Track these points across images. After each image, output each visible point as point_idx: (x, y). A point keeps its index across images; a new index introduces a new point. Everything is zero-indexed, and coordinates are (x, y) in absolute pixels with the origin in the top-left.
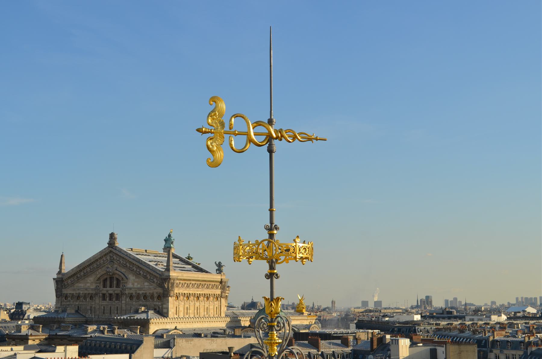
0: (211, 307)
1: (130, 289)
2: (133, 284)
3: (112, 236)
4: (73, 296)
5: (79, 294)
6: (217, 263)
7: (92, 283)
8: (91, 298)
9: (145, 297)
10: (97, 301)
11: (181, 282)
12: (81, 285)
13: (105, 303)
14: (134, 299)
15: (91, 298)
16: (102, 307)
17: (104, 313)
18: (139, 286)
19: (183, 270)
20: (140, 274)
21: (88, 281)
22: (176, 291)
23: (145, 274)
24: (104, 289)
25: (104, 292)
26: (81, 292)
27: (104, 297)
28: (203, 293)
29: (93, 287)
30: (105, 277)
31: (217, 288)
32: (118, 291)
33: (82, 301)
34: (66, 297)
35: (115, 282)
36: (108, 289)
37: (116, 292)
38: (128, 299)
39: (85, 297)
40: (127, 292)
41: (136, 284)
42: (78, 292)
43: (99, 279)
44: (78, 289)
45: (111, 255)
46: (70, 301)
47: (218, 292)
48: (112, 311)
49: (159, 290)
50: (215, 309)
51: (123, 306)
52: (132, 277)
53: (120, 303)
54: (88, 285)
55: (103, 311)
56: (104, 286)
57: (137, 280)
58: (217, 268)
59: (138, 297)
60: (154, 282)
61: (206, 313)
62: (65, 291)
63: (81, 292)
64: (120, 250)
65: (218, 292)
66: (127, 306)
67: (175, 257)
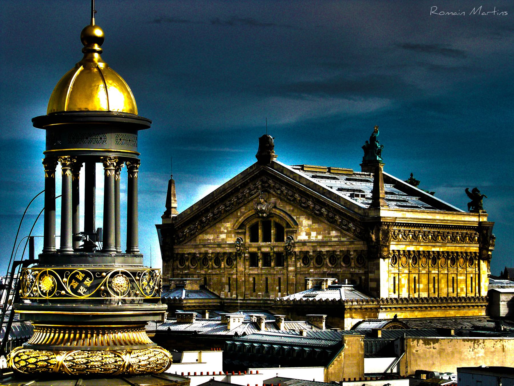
0: (461, 278)
1: (304, 243)
2: (308, 234)
5: (206, 253)
6: (470, 190)
10: (241, 268)
11: (402, 229)
15: (230, 262)
16: (251, 279)
17: (254, 291)
18: (320, 237)
19: (402, 205)
20: (321, 214)
22: (393, 247)
23: (331, 215)
24: (254, 244)
26: (210, 251)
27: (253, 260)
28: (445, 249)
30: (254, 221)
31: (472, 240)
32: (279, 247)
33: (213, 268)
36: (261, 243)
37: (275, 250)
40: (297, 250)
41: (314, 234)
42: (203, 250)
43: (242, 226)
44: (204, 246)
46: (188, 268)
47: (474, 248)
50: (469, 282)
52: (305, 222)
54: (223, 236)
55: (252, 286)
56: (254, 238)
57: (316, 226)
58: (470, 200)
59: (319, 258)
60: (349, 230)
61: (451, 290)
63: (210, 251)
65: (474, 248)
66: (298, 276)
67: (388, 180)
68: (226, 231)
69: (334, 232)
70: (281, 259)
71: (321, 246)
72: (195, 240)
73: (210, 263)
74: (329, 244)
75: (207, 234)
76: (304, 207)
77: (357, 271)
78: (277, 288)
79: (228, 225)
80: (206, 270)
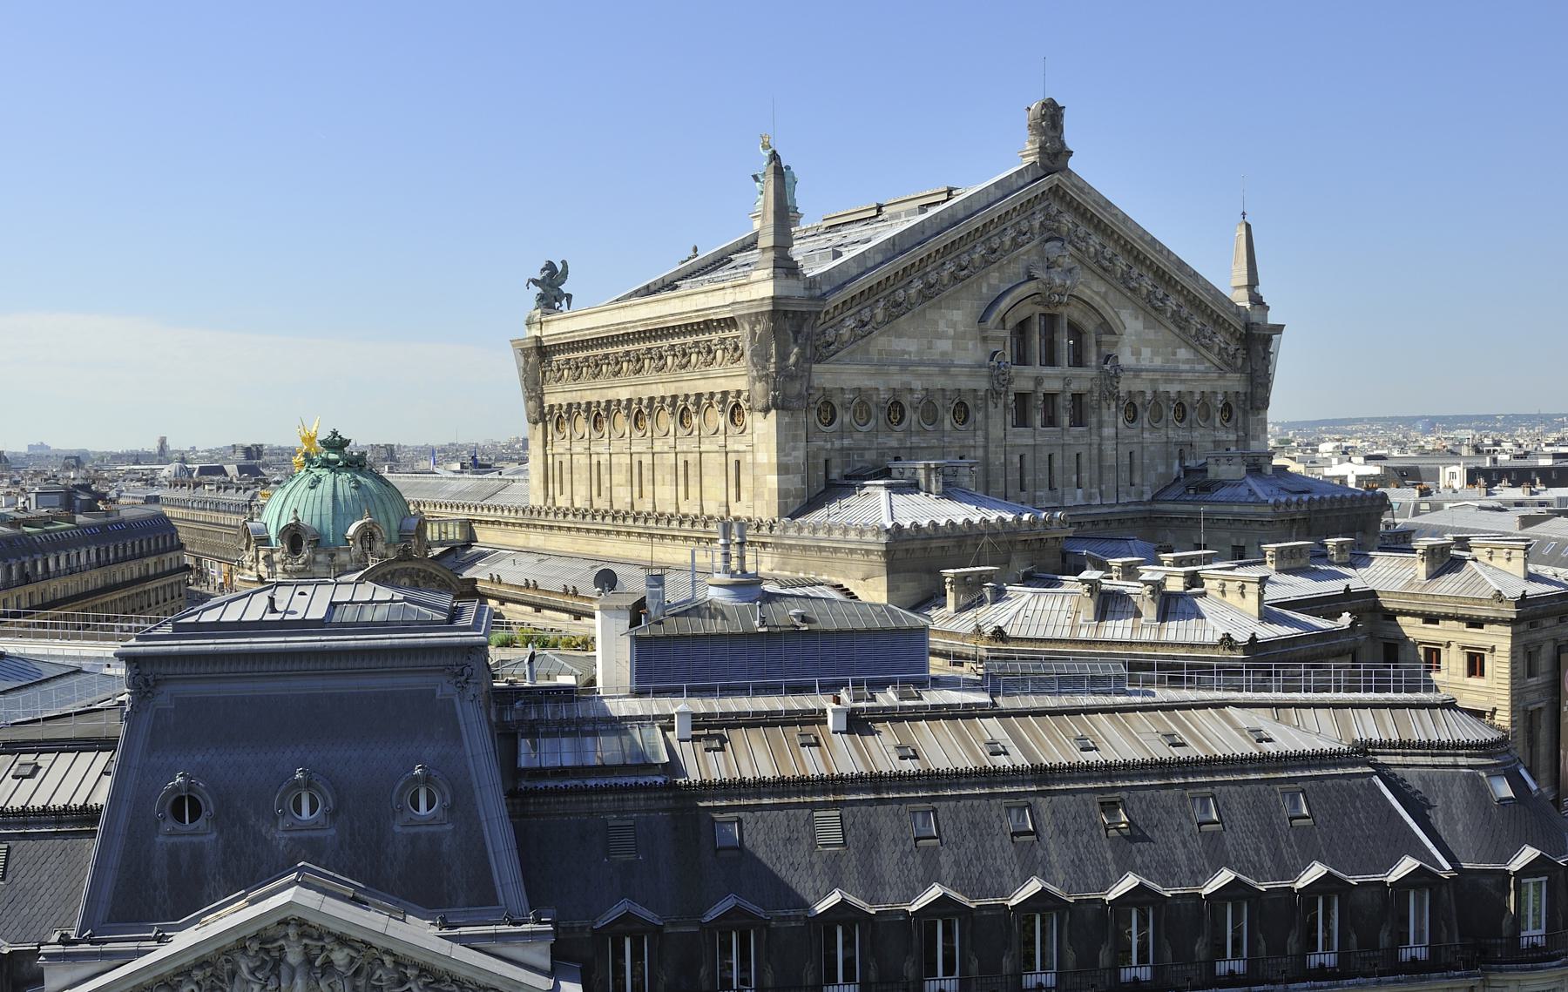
2: (1136, 353)
3: (1051, 118)
4: (862, 403)
7: (963, 336)
8: (962, 412)
9: (1181, 410)
10: (996, 432)
12: (906, 345)
13: (1024, 437)
14: (1146, 417)
15: (962, 412)
16: (1016, 459)
18: (1158, 361)
21: (942, 327)
25: (1025, 385)
26: (917, 384)
29: (972, 353)
30: (1025, 311)
32: (1084, 379)
34: (828, 411)
35: (1065, 342)
37: (1074, 387)
38: (1120, 420)
39: (929, 411)
40: (1123, 388)
41: (1146, 352)
42: (896, 381)
43: (1003, 320)
45: (1055, 208)
48: (1058, 477)
49: (1234, 383)
51: (1109, 448)
52: (1131, 324)
53: (1095, 439)
54: (944, 345)
57: (1151, 334)
62: (827, 376)
64: (1085, 188)
68: (951, 332)
69: (1183, 351)
70: (1080, 409)
71: (1167, 381)
72: (867, 352)
73: (914, 417)
74: (1184, 376)
75: (900, 335)
76: (1133, 290)
77: (1222, 435)
78: (1074, 478)
79: (957, 315)
80: (901, 435)
